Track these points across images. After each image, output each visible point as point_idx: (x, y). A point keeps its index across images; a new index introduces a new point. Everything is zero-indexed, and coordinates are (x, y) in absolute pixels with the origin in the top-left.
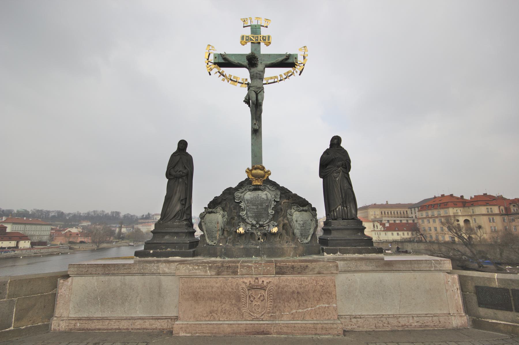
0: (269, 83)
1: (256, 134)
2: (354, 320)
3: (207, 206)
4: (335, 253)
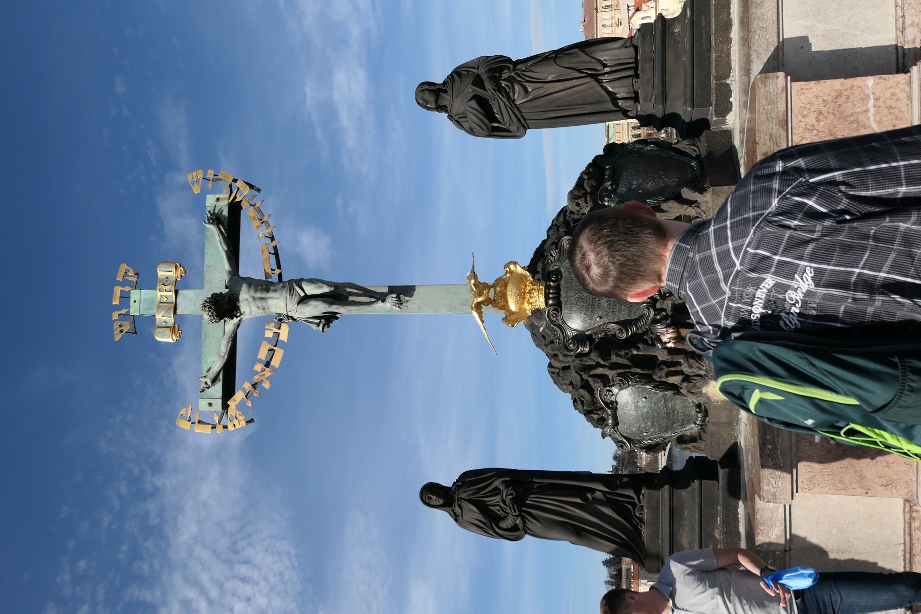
0: (279, 267)
3: (599, 431)
4: (728, 91)
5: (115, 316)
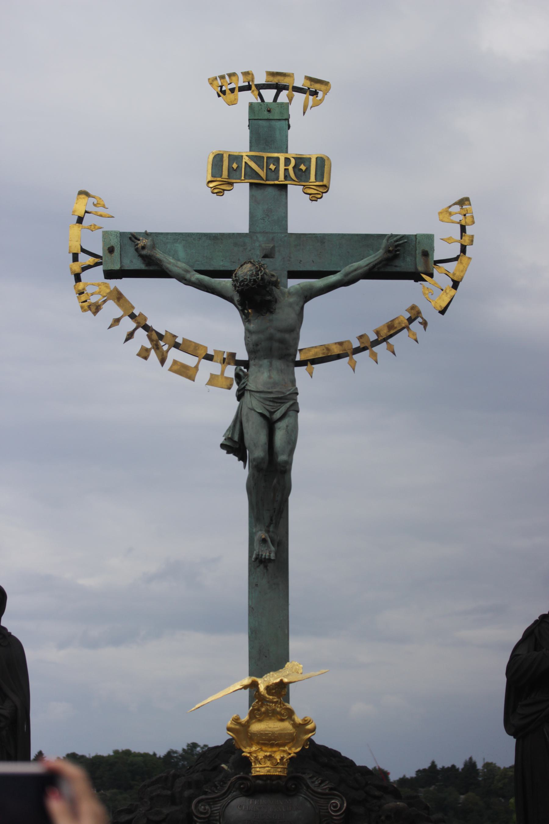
1: (266, 567)
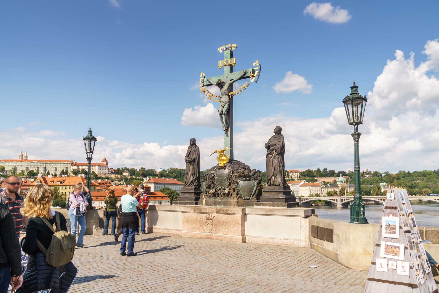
2: (253, 238)
4: (260, 205)
5: (224, 47)
